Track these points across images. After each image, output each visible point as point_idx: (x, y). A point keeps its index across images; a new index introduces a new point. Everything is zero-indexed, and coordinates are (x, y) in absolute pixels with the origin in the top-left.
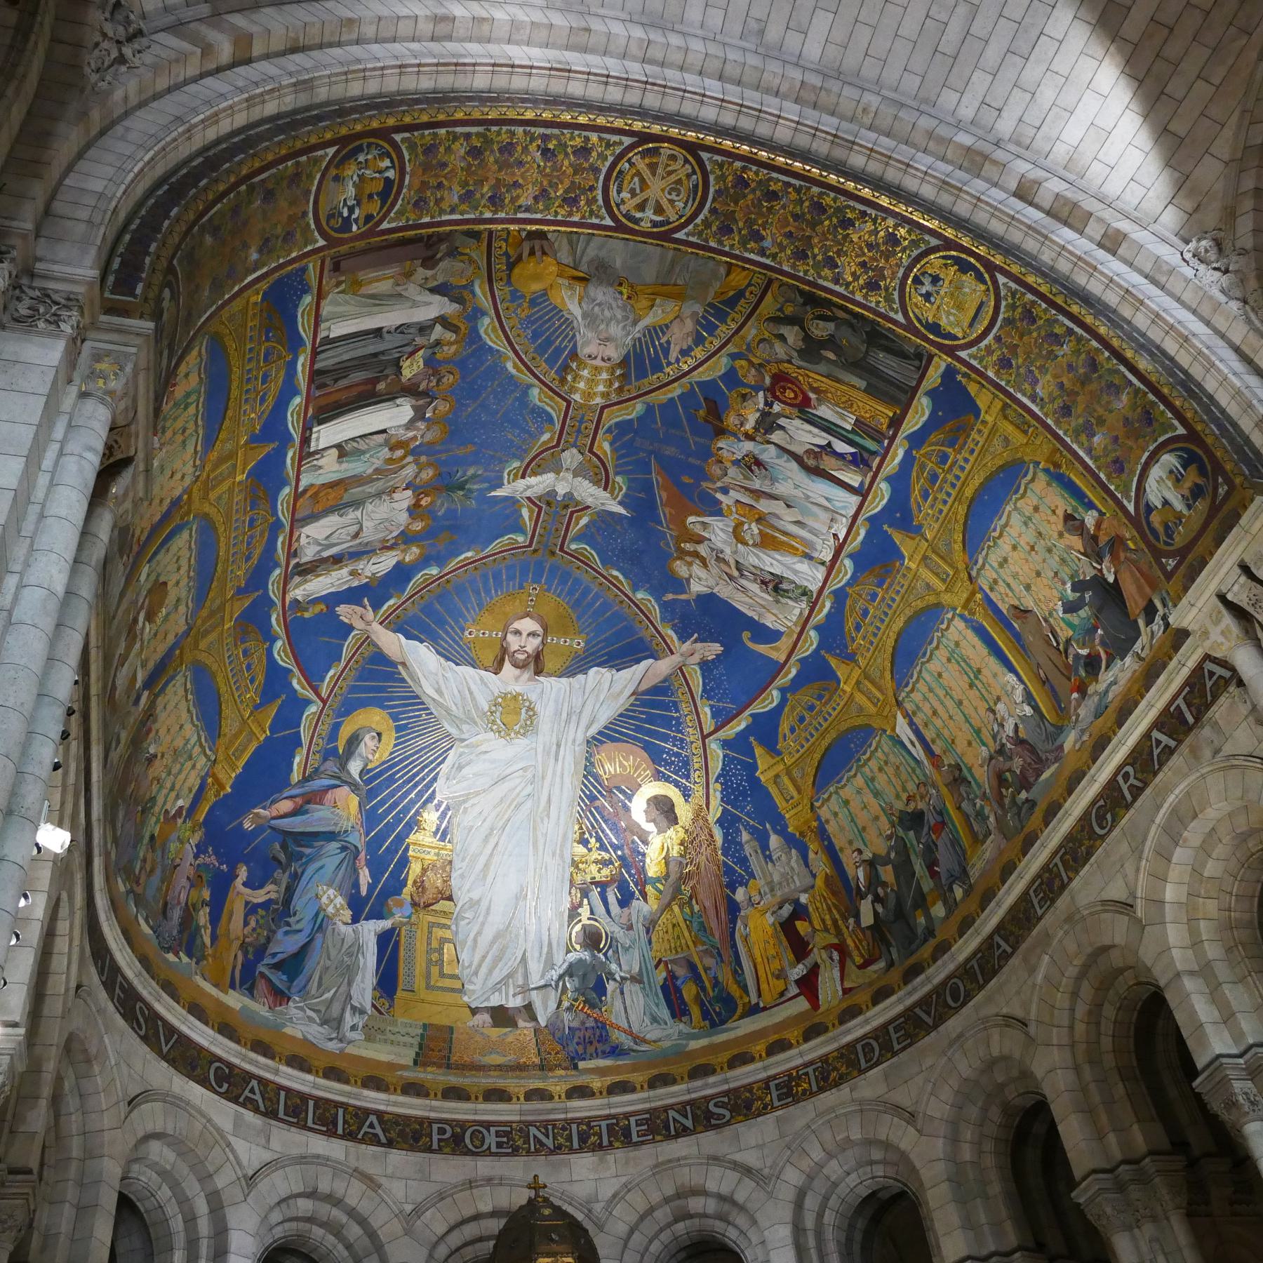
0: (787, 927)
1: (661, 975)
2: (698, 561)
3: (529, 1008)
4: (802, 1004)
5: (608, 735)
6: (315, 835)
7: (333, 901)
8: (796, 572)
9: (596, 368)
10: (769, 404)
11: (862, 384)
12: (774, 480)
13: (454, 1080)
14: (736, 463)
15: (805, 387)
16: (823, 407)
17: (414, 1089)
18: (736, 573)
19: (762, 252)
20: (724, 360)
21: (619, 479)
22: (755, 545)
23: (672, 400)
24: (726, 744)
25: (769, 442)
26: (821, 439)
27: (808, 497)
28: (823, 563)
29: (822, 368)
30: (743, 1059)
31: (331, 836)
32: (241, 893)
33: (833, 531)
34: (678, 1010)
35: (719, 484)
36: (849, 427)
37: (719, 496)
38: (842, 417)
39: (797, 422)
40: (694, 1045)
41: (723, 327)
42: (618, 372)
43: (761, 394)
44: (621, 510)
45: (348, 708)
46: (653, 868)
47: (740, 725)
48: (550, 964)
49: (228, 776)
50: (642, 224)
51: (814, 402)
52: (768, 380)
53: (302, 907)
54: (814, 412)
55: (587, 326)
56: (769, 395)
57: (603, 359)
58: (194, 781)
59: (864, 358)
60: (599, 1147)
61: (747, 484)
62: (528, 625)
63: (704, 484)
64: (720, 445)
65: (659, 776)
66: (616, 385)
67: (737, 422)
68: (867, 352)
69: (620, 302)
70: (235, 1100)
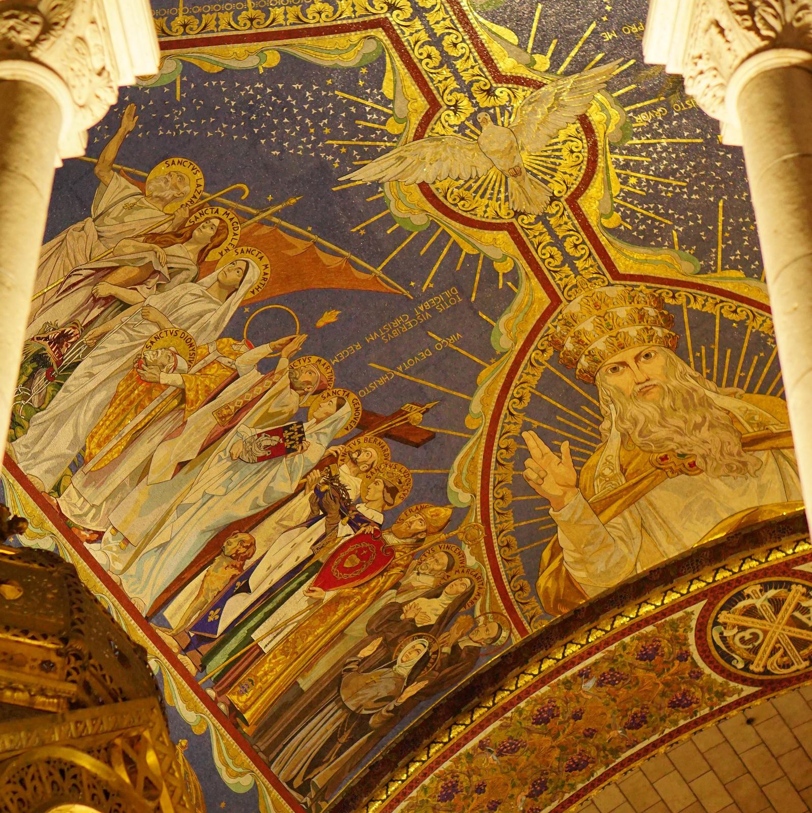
2: (167, 228)
8: (60, 420)
9: (622, 347)
10: (358, 521)
11: (305, 684)
12: (236, 461)
14: (302, 415)
15: (346, 590)
16: (304, 605)
18: (104, 289)
19: (585, 675)
20: (463, 498)
21: (420, 221)
22: (140, 362)
23: (472, 388)
25: (301, 488)
26: (260, 581)
27: (182, 508)
28: (57, 489)
29: (358, 630)
33: (107, 535)
35: (284, 363)
36: (255, 636)
37: (264, 350)
38: (276, 630)
39: (304, 551)
41: (510, 525)
42: (584, 362)
43: (379, 518)
44: (366, 174)
50: (758, 587)
51: (319, 593)
52: (391, 539)
54: (305, 587)
55: (690, 392)
56: (370, 529)
57: (624, 364)
59: (338, 699)
61: (254, 414)
63: (301, 339)
64: (347, 408)
66: (569, 345)
67: (363, 457)
68: (344, 707)
69: (672, 446)
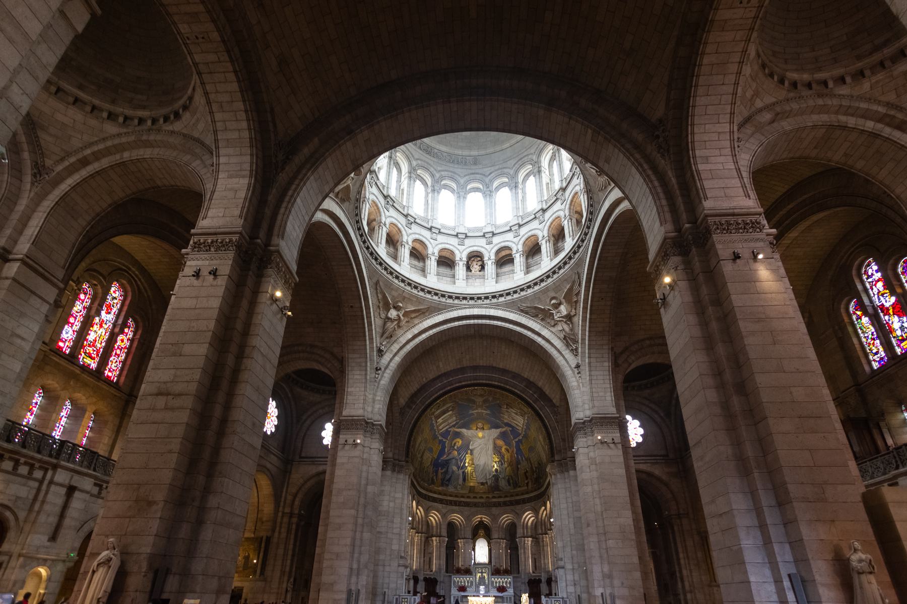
0: (525, 473)
1: (507, 478)
3: (487, 483)
4: (526, 488)
5: (497, 438)
6: (451, 459)
7: (455, 468)
13: (475, 495)
17: (468, 497)
24: (516, 442)
30: (517, 495)
31: (453, 458)
32: (440, 471)
34: (510, 485)
40: (512, 491)
45: (453, 440)
46: (506, 460)
47: (517, 440)
48: (490, 475)
49: (435, 456)
53: (450, 470)
58: (430, 460)
60: (496, 506)
62: (480, 424)
65: (506, 445)
70: (441, 503)
